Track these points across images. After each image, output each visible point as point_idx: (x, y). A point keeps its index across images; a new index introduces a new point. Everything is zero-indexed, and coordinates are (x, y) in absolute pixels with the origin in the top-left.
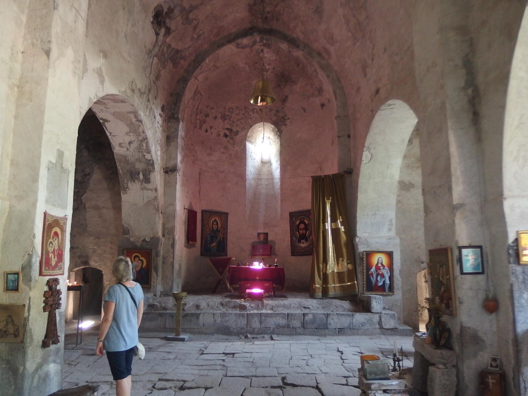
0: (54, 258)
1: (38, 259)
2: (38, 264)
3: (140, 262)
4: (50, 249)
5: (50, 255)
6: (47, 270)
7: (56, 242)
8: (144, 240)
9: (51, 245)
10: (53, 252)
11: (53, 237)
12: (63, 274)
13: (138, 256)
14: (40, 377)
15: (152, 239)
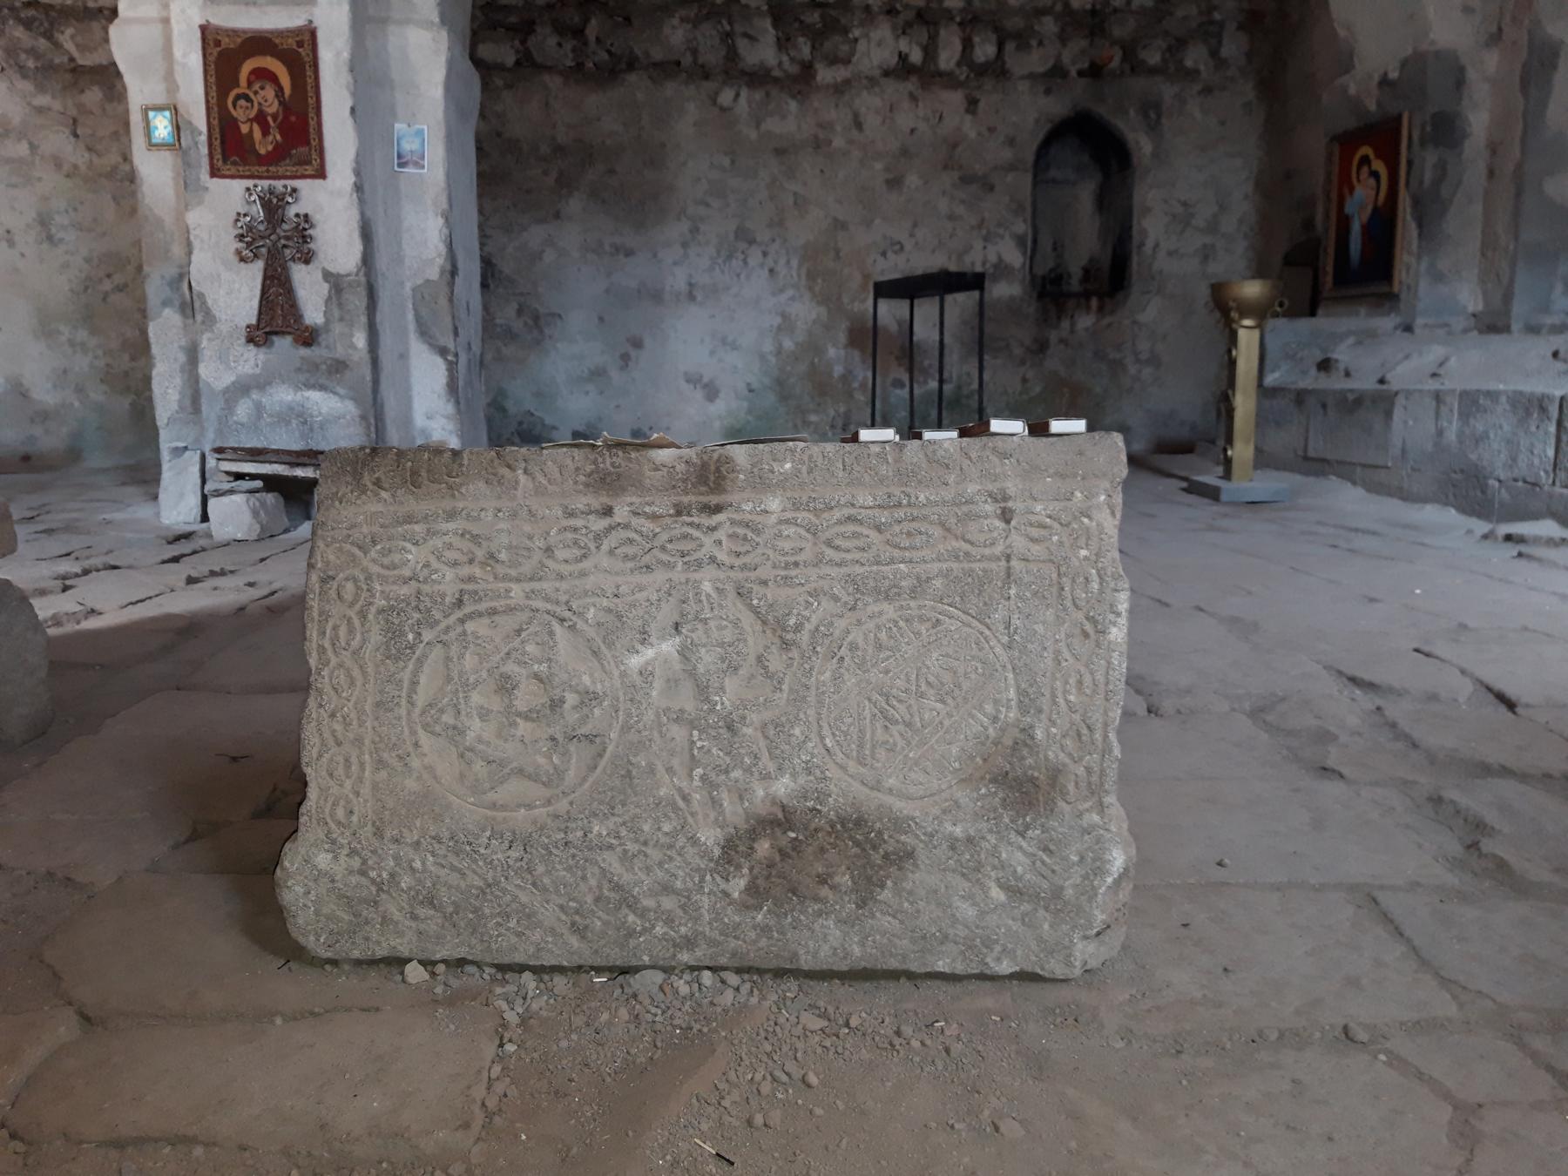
0: (265, 131)
1: (204, 138)
2: (204, 150)
3: (1372, 181)
4: (239, 114)
5: (245, 129)
6: (235, 164)
7: (269, 92)
8: (1384, 82)
9: (242, 102)
10: (261, 118)
11: (250, 84)
12: (321, 174)
13: (1365, 160)
14: (259, 407)
15: (1404, 64)
